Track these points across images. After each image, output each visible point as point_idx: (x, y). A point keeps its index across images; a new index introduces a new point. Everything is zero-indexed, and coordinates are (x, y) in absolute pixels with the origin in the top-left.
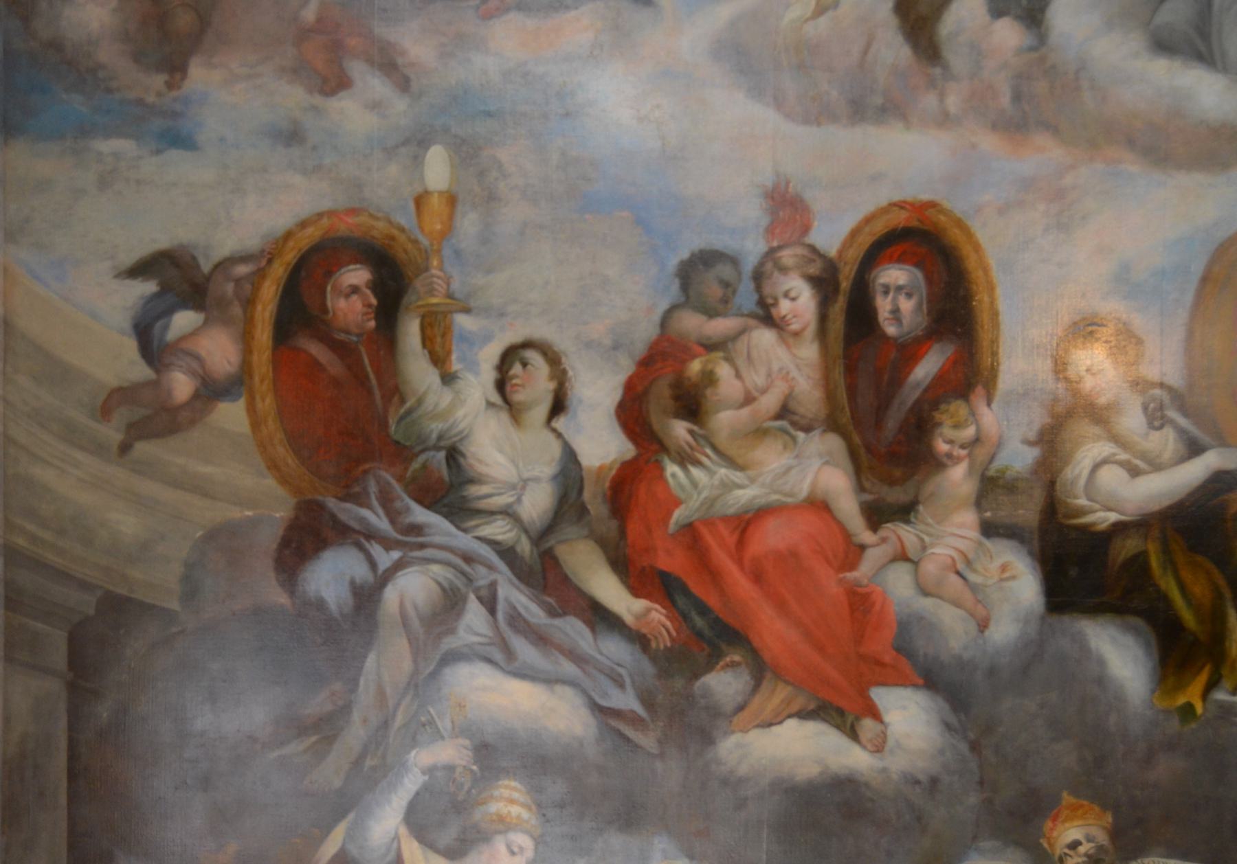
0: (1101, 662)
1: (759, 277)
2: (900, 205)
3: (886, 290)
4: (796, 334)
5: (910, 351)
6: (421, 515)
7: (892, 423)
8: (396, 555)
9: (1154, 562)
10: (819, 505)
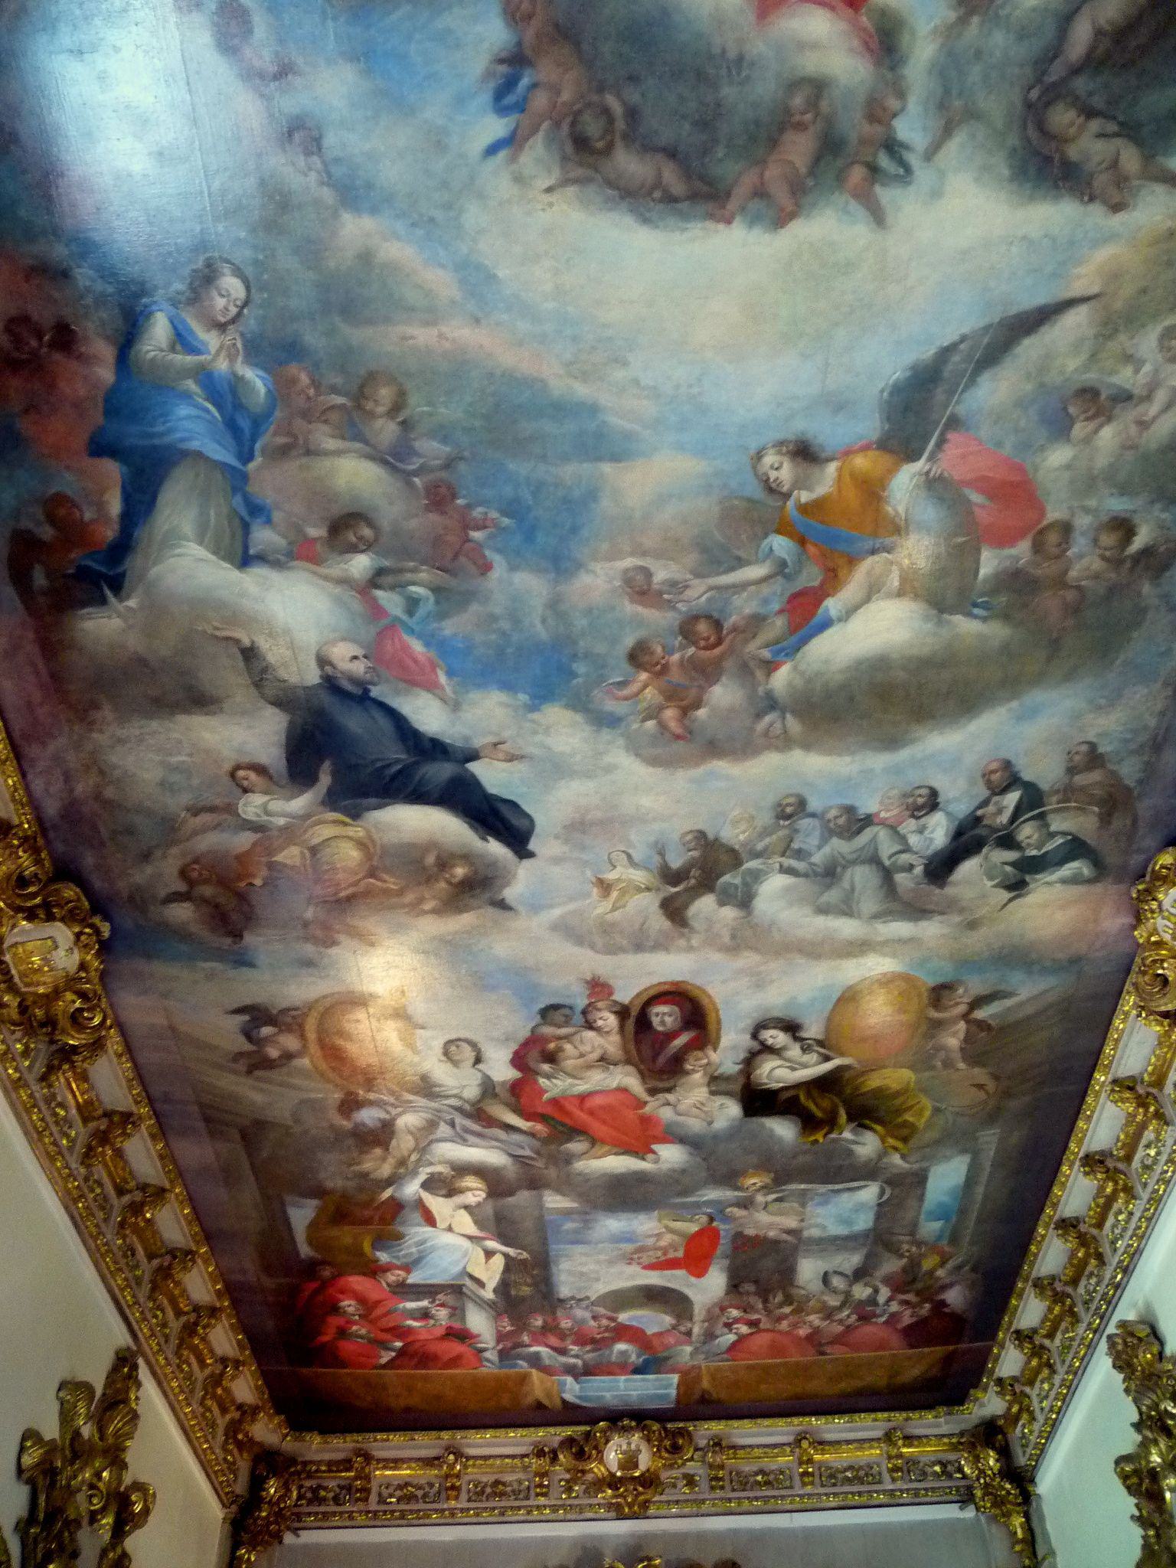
0: (772, 1130)
1: (584, 1012)
2: (665, 983)
3: (657, 1015)
4: (608, 1032)
5: (672, 1035)
7: (661, 1060)
8: (400, 1109)
9: (802, 1098)
10: (623, 1090)
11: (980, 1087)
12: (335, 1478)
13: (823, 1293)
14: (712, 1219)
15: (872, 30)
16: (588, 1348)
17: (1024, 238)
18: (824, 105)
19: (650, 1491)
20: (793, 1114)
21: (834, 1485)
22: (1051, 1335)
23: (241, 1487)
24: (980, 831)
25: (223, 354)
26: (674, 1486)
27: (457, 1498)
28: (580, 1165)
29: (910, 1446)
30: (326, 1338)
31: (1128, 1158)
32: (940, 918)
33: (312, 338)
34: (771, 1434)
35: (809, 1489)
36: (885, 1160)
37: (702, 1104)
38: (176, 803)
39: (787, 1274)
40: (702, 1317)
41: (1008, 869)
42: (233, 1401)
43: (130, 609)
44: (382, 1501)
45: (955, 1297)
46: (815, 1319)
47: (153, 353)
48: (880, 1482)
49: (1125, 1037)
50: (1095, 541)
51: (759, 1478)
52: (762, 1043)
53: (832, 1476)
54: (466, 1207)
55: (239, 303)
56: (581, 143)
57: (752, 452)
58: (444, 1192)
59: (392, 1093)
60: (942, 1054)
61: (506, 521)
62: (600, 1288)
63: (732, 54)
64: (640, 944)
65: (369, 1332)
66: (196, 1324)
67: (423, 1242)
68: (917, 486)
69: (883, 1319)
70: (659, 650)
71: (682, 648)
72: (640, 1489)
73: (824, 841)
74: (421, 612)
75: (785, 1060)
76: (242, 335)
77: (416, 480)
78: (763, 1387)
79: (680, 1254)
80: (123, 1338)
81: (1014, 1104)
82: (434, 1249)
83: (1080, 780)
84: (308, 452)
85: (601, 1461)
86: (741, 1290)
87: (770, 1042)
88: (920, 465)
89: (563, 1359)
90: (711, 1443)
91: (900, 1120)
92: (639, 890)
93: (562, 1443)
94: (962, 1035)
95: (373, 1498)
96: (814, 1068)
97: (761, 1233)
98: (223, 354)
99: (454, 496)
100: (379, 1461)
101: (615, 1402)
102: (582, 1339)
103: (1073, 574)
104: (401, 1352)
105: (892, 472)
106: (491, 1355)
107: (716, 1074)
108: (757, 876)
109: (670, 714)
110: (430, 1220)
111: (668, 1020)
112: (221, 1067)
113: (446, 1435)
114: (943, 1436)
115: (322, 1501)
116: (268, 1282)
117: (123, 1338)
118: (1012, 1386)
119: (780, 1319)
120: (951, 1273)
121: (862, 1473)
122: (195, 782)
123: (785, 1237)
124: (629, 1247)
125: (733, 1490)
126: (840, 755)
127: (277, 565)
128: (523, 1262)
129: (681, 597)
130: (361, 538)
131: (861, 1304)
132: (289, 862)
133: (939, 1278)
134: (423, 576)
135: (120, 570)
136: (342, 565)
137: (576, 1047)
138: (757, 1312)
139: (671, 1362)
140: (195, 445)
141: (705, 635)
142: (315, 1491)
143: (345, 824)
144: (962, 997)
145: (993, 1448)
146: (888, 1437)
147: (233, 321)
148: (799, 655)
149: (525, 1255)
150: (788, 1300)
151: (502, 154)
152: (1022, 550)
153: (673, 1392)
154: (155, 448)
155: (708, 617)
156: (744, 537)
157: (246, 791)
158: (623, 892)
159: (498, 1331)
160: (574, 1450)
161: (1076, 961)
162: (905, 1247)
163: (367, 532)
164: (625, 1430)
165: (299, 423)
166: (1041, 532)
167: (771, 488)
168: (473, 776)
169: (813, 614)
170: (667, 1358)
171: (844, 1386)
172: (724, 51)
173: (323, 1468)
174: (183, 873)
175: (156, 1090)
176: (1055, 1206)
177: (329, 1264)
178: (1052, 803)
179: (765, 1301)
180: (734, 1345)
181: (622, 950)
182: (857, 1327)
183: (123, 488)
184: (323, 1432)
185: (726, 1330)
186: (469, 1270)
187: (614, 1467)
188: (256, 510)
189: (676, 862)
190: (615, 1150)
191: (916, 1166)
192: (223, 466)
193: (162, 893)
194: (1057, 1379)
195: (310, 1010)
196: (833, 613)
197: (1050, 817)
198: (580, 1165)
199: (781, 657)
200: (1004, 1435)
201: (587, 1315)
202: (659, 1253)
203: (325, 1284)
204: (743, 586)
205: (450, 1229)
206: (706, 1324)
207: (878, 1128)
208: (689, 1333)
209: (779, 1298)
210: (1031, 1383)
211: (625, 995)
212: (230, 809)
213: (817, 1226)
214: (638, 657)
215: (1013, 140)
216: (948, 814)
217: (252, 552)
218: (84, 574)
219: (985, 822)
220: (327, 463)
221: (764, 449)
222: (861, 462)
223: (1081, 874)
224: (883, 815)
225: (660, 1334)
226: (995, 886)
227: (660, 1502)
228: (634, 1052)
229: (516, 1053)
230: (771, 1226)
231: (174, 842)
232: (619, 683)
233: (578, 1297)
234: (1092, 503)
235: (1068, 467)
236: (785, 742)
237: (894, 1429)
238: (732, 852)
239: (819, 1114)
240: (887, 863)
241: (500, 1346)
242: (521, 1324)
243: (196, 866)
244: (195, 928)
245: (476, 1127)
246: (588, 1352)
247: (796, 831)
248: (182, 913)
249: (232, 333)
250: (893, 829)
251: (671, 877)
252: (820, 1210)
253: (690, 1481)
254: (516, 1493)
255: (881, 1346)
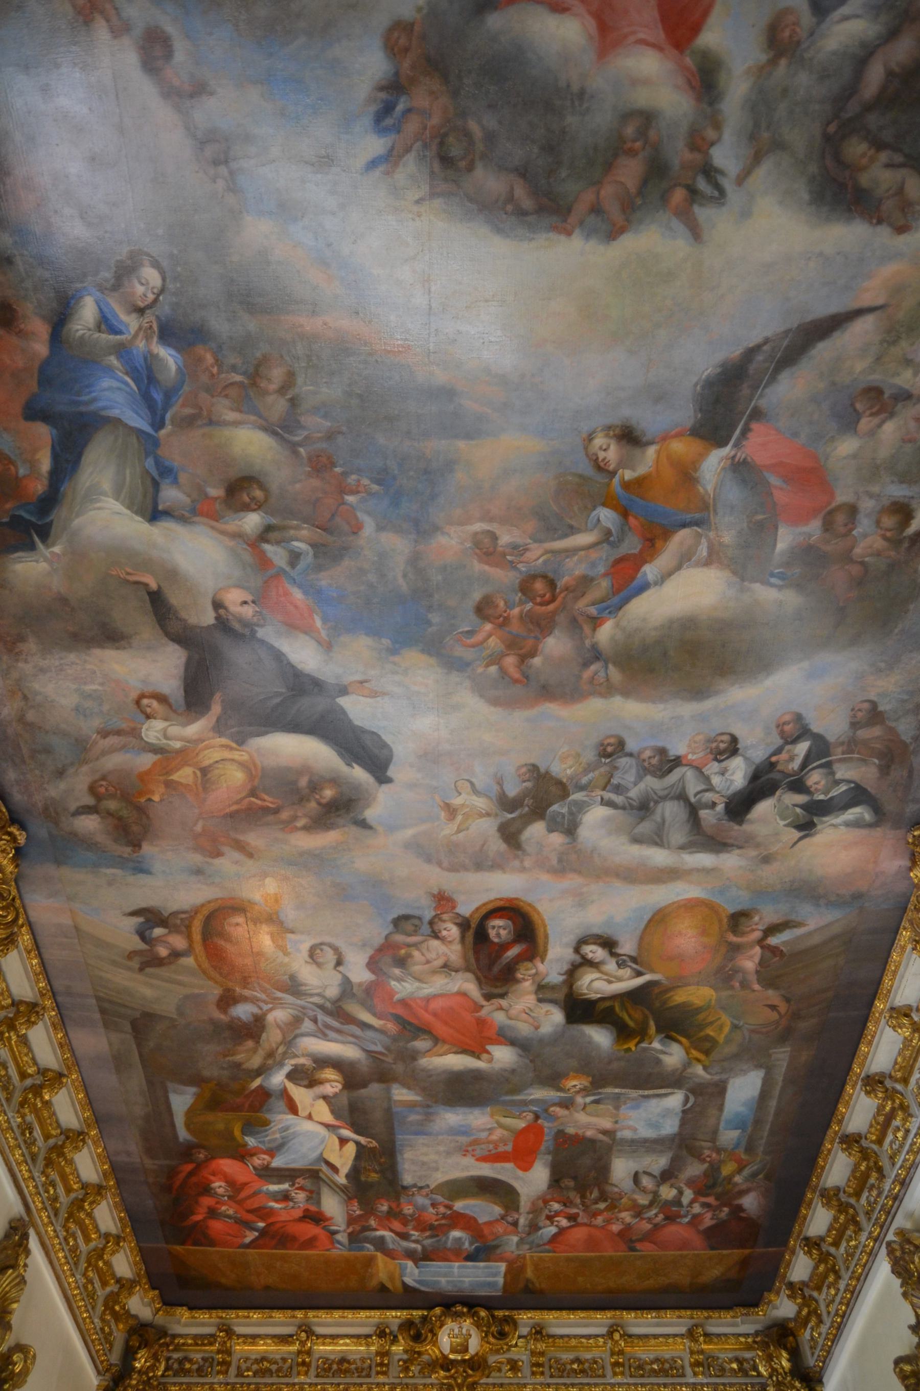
0: (590, 1037)
1: (431, 923)
2: (501, 899)
3: (494, 927)
4: (450, 942)
5: (505, 947)
6: (279, 994)
7: (496, 969)
8: (271, 1006)
9: (617, 1009)
10: (463, 994)
11: (773, 1007)
12: (200, 1351)
13: (634, 1192)
14: (537, 1117)
15: (693, 68)
16: (428, 1233)
17: (821, 254)
18: (652, 134)
19: (478, 1374)
20: (608, 1023)
21: (642, 1376)
22: (836, 1244)
23: (115, 1357)
24: (774, 775)
25: (141, 334)
26: (500, 1370)
27: (306, 1373)
28: (424, 1062)
29: (710, 1342)
30: (198, 1217)
31: (905, 1081)
32: (737, 851)
33: (219, 325)
34: (586, 1326)
35: (619, 1379)
36: (689, 1070)
37: (530, 1009)
38: (89, 726)
39: (603, 1171)
40: (527, 1209)
41: (798, 810)
42: (113, 1275)
43: (53, 553)
44: (240, 1374)
45: (750, 1202)
46: (626, 1216)
47: (81, 332)
48: (683, 1375)
49: (902, 968)
50: (878, 523)
51: (575, 1366)
52: (583, 957)
53: (640, 1367)
54: (325, 1098)
55: (155, 291)
56: (446, 160)
57: (584, 435)
58: (305, 1082)
59: (264, 991)
60: (739, 976)
61: (375, 487)
62: (439, 1177)
63: (575, 88)
64: (481, 863)
65: (236, 1212)
66: (83, 1201)
67: (286, 1128)
68: (724, 469)
69: (686, 1220)
70: (502, 604)
71: (521, 603)
72: (470, 1372)
73: (640, 778)
74: (302, 565)
75: (602, 972)
76: (158, 317)
77: (301, 450)
78: (580, 1279)
79: (509, 1148)
80: (18, 1208)
81: (803, 1026)
82: (295, 1135)
83: (863, 734)
84: (211, 423)
85: (435, 1343)
86: (563, 1185)
87: (590, 956)
88: (727, 451)
89: (405, 1244)
90: (534, 1331)
91: (702, 1034)
92: (481, 815)
93: (401, 1326)
94: (757, 959)
95: (233, 1371)
96: (627, 982)
97: (580, 1132)
98: (141, 334)
99: (333, 465)
100: (239, 1336)
101: (450, 1288)
102: (423, 1226)
103: (858, 551)
104: (263, 1233)
105: (702, 456)
106: (342, 1237)
107: (543, 983)
108: (582, 807)
109: (510, 661)
110: (293, 1108)
111: (503, 933)
112: (114, 963)
113: (300, 1314)
114: (740, 1335)
115: (187, 1372)
116: (149, 1163)
117: (18, 1208)
118: (801, 1290)
119: (595, 1214)
120: (746, 1180)
121: (667, 1366)
122: (106, 708)
123: (601, 1137)
124: (464, 1140)
125: (552, 1376)
126: (654, 702)
127: (183, 520)
128: (372, 1150)
129: (522, 559)
130: (253, 499)
131: (667, 1204)
132: (183, 781)
133: (736, 1184)
134: (304, 533)
135: (48, 520)
136: (236, 522)
137: (423, 955)
138: (576, 1206)
139: (498, 1251)
140: (115, 413)
141: (541, 592)
142: (181, 1362)
143: (231, 749)
144: (759, 922)
145: (786, 1349)
146: (691, 1334)
147: (149, 307)
148: (621, 613)
149: (374, 1144)
150: (603, 1197)
151: (382, 168)
152: (814, 527)
153: (500, 1280)
154: (82, 414)
155: (545, 577)
156: (576, 508)
157: (148, 717)
158: (467, 816)
159: (349, 1215)
160: (412, 1333)
161: (858, 896)
162: (707, 1152)
163: (258, 494)
164: (458, 1315)
165: (203, 396)
166: (830, 513)
167: (599, 466)
168: (344, 712)
169: (633, 578)
170: (496, 1247)
171: (650, 1283)
172: (568, 86)
173: (190, 1341)
174: (92, 789)
175: (59, 985)
176: (840, 1122)
177: (203, 1147)
178: (837, 754)
179: (583, 1197)
180: (555, 1236)
181: (466, 869)
182: (664, 1226)
183: (53, 447)
184: (191, 1308)
185: (548, 1222)
186: (325, 1156)
187: (446, 1350)
188: (166, 472)
189: (512, 790)
190: (454, 1049)
191: (717, 1078)
192: (139, 432)
193: (73, 807)
194: (842, 1285)
195: (196, 913)
196: (650, 577)
197: (836, 766)
198: (424, 1062)
199: (604, 615)
200: (794, 1336)
201: (427, 1202)
202: (491, 1147)
203: (199, 1166)
204: (574, 551)
205: (310, 1117)
206: (531, 1216)
207: (683, 1040)
208: (515, 1224)
209: (595, 1194)
210: (819, 1288)
211: (466, 908)
212: (135, 733)
213: (629, 1128)
214: (483, 610)
215: (813, 168)
216: (746, 759)
217: (160, 508)
218: (16, 522)
219: (779, 767)
220: (227, 432)
221: (594, 432)
222: (678, 447)
223: (863, 819)
224: (690, 757)
225: (489, 1223)
226: (785, 826)
227: (487, 1384)
228: (472, 960)
229: (371, 958)
230: (588, 1126)
231: (85, 762)
232: (468, 632)
233: (419, 1185)
234: (876, 489)
235: (854, 456)
236: (608, 690)
237: (696, 1326)
238: (560, 783)
239: (631, 1024)
240: (693, 800)
241: (350, 1230)
242: (369, 1210)
243: (104, 783)
244: (101, 838)
245: (335, 1024)
246: (427, 1238)
247: (616, 768)
248: (89, 824)
249: (149, 317)
250: (699, 770)
251: (507, 804)
252: (633, 1114)
253: (514, 1366)
254: (359, 1371)
255: (685, 1245)
